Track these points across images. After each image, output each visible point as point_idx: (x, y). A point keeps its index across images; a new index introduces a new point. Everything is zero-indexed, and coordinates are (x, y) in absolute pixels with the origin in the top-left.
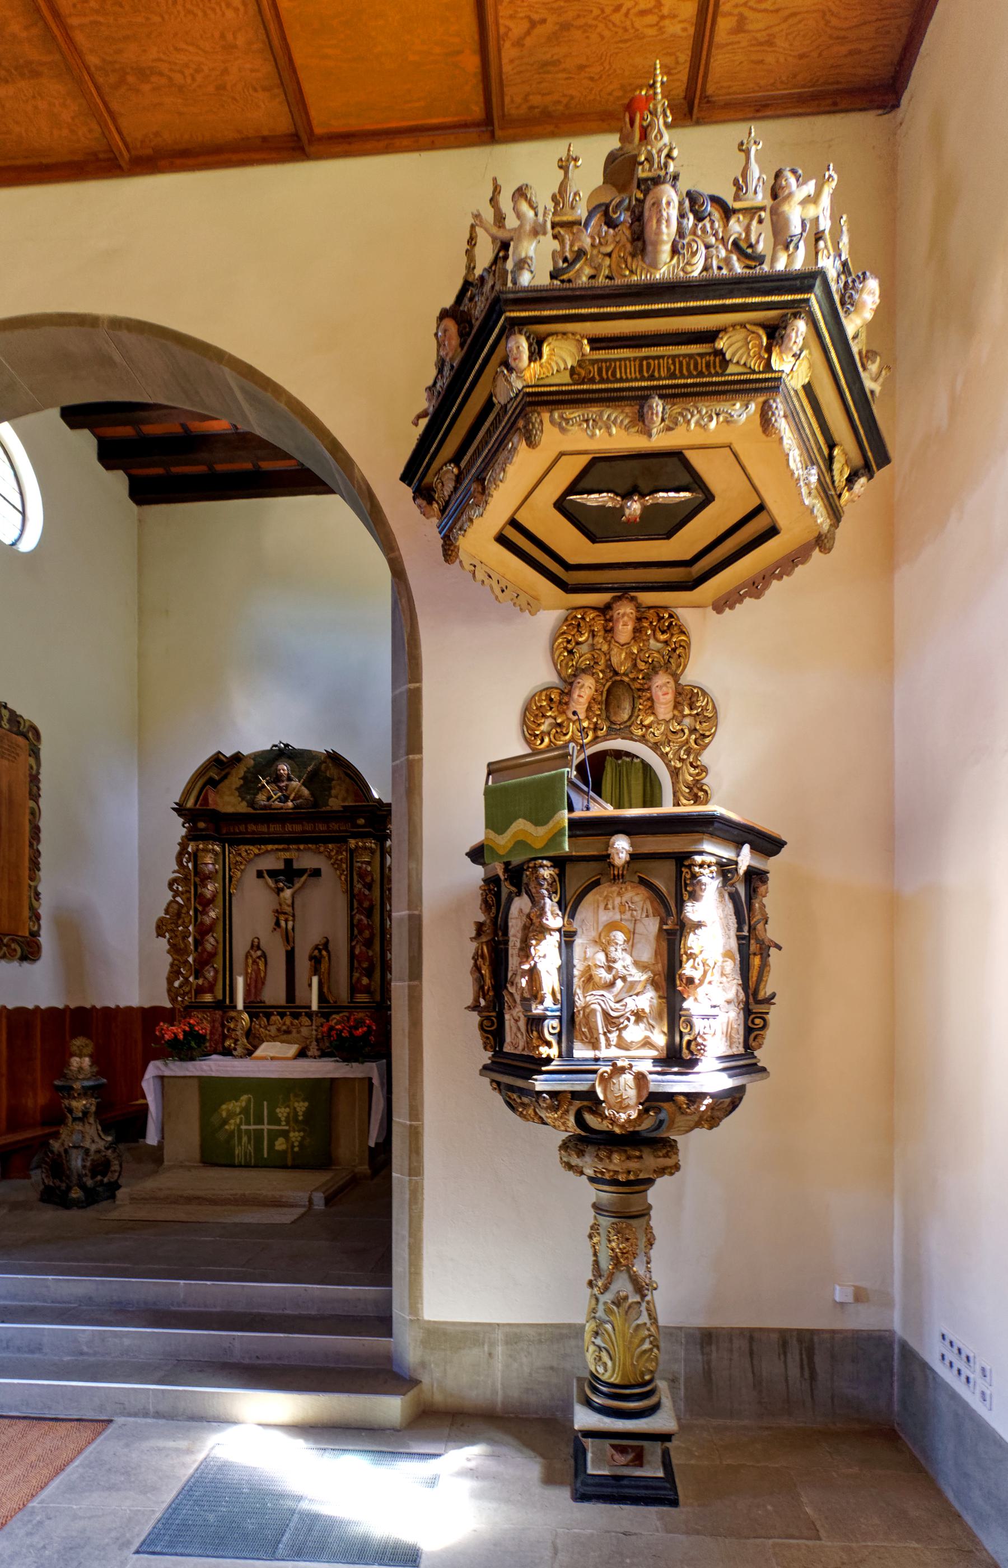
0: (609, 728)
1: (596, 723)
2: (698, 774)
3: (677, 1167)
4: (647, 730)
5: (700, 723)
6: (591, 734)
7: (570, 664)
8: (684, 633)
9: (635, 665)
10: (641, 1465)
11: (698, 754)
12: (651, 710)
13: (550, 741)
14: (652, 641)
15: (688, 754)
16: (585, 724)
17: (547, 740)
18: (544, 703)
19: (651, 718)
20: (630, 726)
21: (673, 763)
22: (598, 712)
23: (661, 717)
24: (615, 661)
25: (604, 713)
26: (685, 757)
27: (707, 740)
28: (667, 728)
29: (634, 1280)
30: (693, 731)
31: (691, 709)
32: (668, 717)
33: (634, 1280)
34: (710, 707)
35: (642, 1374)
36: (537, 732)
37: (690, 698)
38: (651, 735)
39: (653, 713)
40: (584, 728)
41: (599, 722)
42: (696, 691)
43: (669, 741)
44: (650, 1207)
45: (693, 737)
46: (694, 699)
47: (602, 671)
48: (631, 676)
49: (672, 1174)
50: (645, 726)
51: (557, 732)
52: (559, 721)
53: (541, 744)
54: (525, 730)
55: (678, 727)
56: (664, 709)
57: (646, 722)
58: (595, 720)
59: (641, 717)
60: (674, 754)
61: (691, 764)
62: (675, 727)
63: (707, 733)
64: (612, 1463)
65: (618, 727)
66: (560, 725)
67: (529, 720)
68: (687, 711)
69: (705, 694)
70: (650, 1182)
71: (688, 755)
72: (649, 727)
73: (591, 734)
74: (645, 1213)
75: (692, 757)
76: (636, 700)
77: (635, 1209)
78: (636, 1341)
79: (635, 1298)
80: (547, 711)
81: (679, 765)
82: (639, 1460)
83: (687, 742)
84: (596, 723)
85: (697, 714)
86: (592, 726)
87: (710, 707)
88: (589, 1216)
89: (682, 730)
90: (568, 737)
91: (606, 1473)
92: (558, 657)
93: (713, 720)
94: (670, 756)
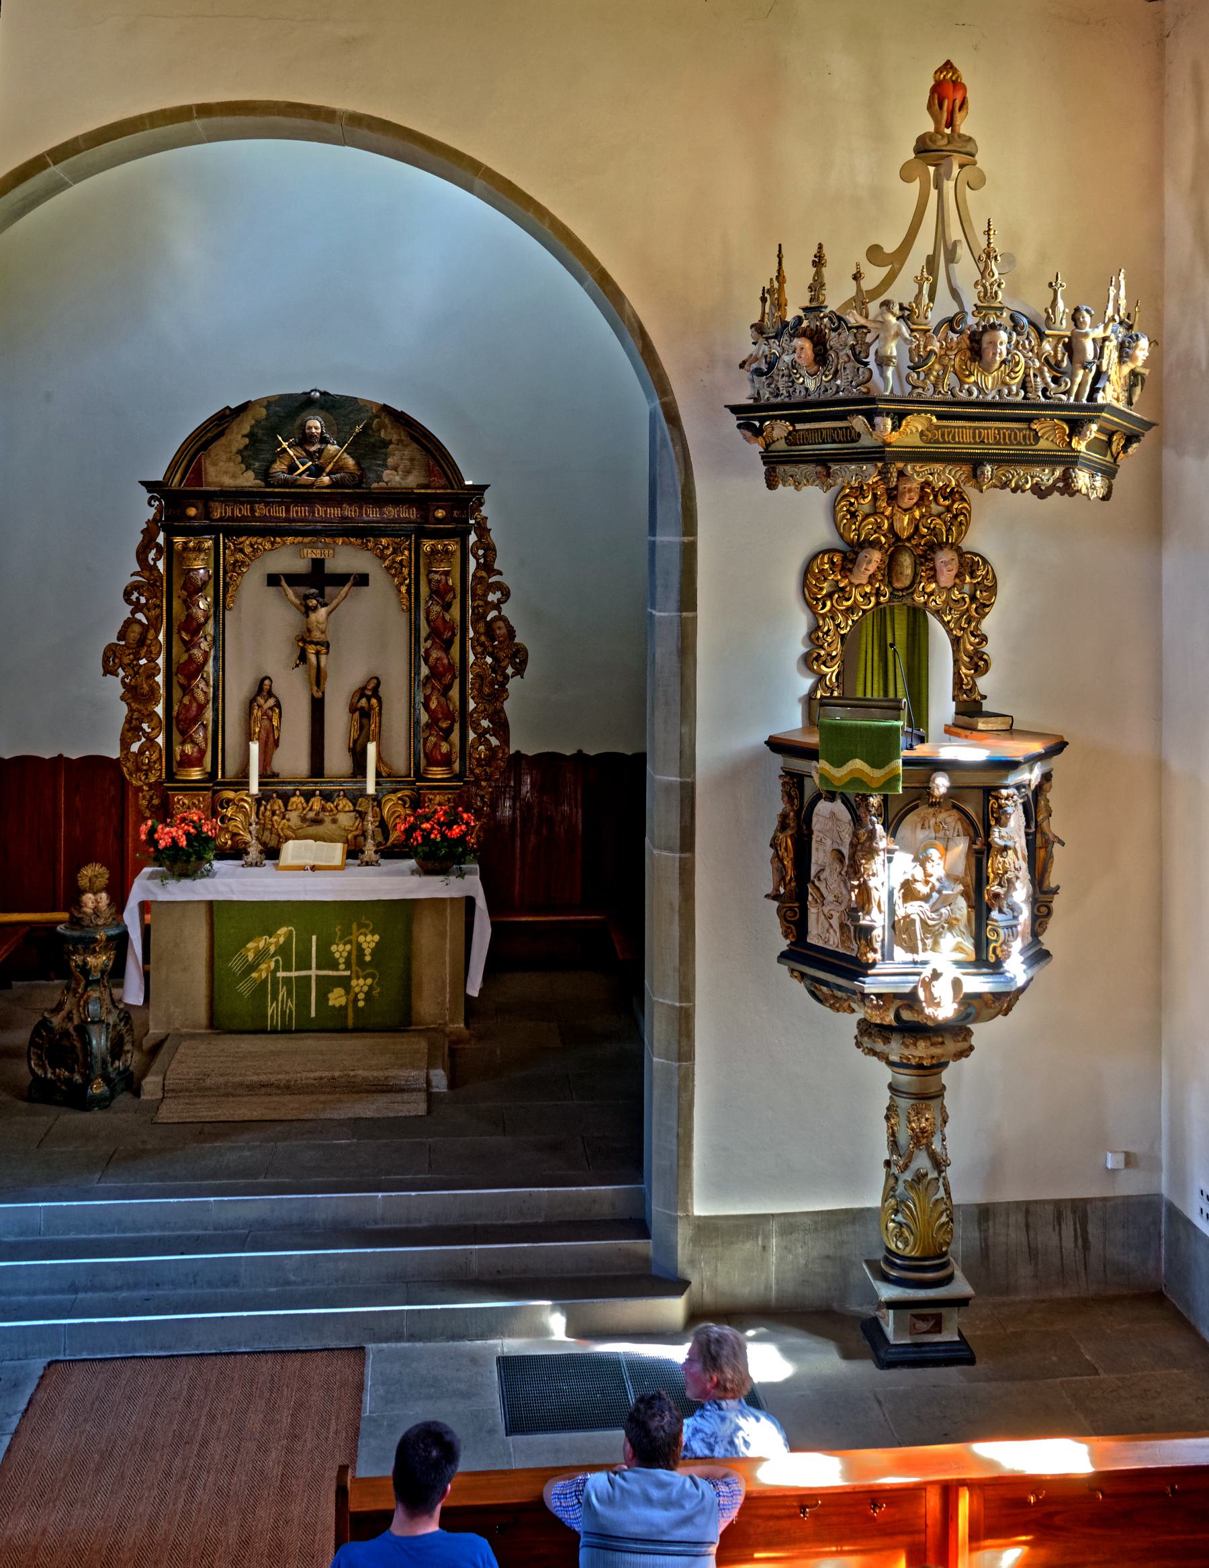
0: (891, 594)
1: (878, 589)
2: (979, 643)
3: (971, 1048)
4: (929, 597)
5: (981, 592)
6: (873, 599)
7: (854, 527)
8: (963, 499)
9: (917, 528)
10: (940, 1332)
11: (979, 622)
12: (933, 578)
13: (832, 605)
14: (933, 505)
15: (969, 622)
16: (868, 589)
17: (829, 603)
18: (826, 566)
19: (933, 586)
20: (912, 593)
21: (954, 632)
22: (880, 578)
23: (943, 585)
24: (897, 526)
25: (887, 579)
26: (966, 626)
27: (987, 610)
28: (948, 596)
29: (933, 1156)
30: (973, 598)
31: (972, 577)
32: (949, 585)
33: (933, 1156)
34: (990, 576)
35: (941, 1246)
36: (819, 596)
37: (971, 566)
38: (933, 603)
39: (936, 582)
40: (866, 593)
41: (882, 588)
42: (976, 559)
43: (951, 609)
44: (944, 1087)
45: (974, 606)
46: (975, 568)
47: (884, 535)
48: (914, 542)
49: (967, 1056)
50: (926, 593)
51: (839, 597)
52: (842, 585)
53: (822, 609)
54: (807, 593)
55: (959, 596)
56: (946, 578)
57: (928, 590)
58: (877, 585)
59: (922, 584)
60: (955, 624)
61: (972, 633)
62: (956, 595)
63: (988, 603)
64: (913, 1331)
65: (900, 594)
66: (842, 589)
67: (811, 583)
68: (968, 579)
69: (985, 561)
70: (945, 1065)
71: (969, 622)
72: (931, 594)
73: (873, 599)
74: (939, 1094)
75: (973, 624)
76: (918, 566)
77: (933, 1090)
78: (936, 1215)
79: (933, 1175)
80: (830, 575)
81: (959, 633)
82: (937, 1328)
83: (968, 610)
84: (878, 589)
85: (978, 583)
86: (874, 591)
87: (990, 576)
88: (885, 1097)
89: (963, 598)
90: (849, 603)
91: (908, 1342)
92: (841, 521)
93: (992, 590)
94: (952, 625)
